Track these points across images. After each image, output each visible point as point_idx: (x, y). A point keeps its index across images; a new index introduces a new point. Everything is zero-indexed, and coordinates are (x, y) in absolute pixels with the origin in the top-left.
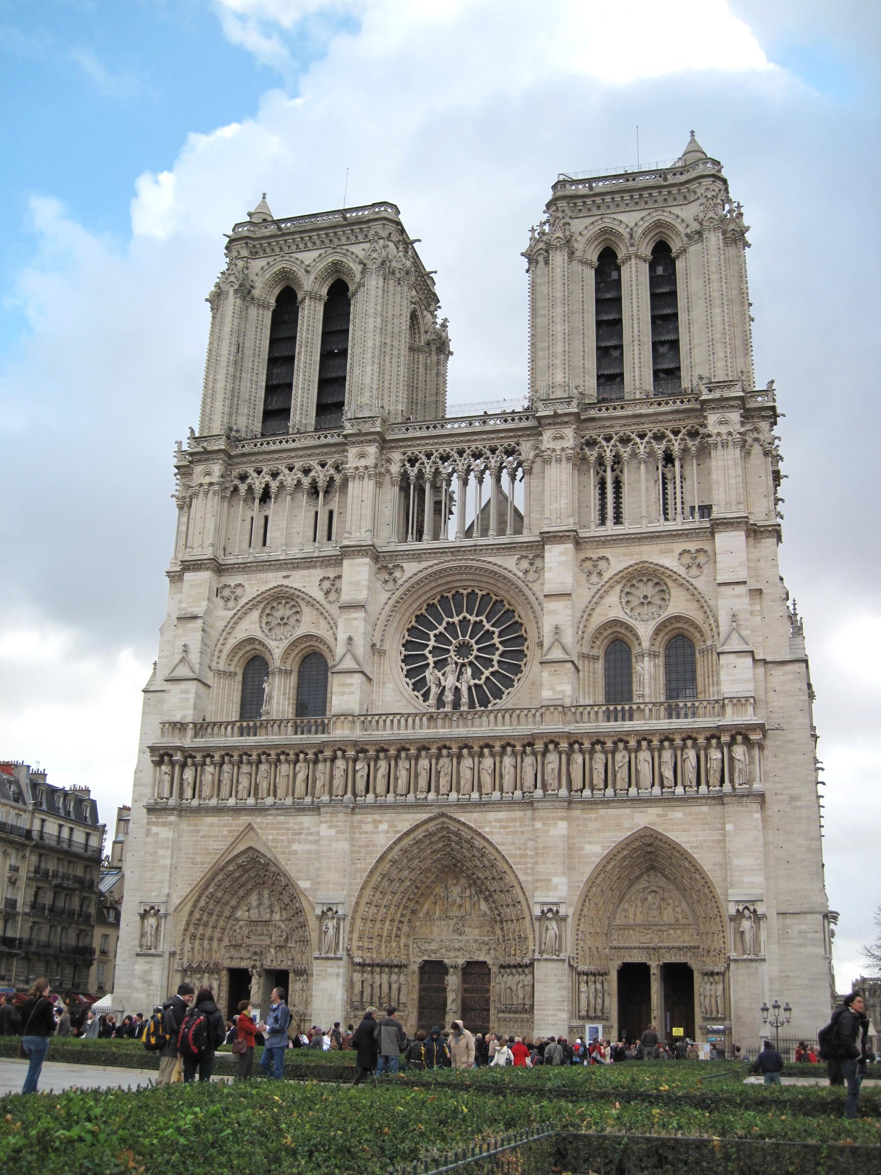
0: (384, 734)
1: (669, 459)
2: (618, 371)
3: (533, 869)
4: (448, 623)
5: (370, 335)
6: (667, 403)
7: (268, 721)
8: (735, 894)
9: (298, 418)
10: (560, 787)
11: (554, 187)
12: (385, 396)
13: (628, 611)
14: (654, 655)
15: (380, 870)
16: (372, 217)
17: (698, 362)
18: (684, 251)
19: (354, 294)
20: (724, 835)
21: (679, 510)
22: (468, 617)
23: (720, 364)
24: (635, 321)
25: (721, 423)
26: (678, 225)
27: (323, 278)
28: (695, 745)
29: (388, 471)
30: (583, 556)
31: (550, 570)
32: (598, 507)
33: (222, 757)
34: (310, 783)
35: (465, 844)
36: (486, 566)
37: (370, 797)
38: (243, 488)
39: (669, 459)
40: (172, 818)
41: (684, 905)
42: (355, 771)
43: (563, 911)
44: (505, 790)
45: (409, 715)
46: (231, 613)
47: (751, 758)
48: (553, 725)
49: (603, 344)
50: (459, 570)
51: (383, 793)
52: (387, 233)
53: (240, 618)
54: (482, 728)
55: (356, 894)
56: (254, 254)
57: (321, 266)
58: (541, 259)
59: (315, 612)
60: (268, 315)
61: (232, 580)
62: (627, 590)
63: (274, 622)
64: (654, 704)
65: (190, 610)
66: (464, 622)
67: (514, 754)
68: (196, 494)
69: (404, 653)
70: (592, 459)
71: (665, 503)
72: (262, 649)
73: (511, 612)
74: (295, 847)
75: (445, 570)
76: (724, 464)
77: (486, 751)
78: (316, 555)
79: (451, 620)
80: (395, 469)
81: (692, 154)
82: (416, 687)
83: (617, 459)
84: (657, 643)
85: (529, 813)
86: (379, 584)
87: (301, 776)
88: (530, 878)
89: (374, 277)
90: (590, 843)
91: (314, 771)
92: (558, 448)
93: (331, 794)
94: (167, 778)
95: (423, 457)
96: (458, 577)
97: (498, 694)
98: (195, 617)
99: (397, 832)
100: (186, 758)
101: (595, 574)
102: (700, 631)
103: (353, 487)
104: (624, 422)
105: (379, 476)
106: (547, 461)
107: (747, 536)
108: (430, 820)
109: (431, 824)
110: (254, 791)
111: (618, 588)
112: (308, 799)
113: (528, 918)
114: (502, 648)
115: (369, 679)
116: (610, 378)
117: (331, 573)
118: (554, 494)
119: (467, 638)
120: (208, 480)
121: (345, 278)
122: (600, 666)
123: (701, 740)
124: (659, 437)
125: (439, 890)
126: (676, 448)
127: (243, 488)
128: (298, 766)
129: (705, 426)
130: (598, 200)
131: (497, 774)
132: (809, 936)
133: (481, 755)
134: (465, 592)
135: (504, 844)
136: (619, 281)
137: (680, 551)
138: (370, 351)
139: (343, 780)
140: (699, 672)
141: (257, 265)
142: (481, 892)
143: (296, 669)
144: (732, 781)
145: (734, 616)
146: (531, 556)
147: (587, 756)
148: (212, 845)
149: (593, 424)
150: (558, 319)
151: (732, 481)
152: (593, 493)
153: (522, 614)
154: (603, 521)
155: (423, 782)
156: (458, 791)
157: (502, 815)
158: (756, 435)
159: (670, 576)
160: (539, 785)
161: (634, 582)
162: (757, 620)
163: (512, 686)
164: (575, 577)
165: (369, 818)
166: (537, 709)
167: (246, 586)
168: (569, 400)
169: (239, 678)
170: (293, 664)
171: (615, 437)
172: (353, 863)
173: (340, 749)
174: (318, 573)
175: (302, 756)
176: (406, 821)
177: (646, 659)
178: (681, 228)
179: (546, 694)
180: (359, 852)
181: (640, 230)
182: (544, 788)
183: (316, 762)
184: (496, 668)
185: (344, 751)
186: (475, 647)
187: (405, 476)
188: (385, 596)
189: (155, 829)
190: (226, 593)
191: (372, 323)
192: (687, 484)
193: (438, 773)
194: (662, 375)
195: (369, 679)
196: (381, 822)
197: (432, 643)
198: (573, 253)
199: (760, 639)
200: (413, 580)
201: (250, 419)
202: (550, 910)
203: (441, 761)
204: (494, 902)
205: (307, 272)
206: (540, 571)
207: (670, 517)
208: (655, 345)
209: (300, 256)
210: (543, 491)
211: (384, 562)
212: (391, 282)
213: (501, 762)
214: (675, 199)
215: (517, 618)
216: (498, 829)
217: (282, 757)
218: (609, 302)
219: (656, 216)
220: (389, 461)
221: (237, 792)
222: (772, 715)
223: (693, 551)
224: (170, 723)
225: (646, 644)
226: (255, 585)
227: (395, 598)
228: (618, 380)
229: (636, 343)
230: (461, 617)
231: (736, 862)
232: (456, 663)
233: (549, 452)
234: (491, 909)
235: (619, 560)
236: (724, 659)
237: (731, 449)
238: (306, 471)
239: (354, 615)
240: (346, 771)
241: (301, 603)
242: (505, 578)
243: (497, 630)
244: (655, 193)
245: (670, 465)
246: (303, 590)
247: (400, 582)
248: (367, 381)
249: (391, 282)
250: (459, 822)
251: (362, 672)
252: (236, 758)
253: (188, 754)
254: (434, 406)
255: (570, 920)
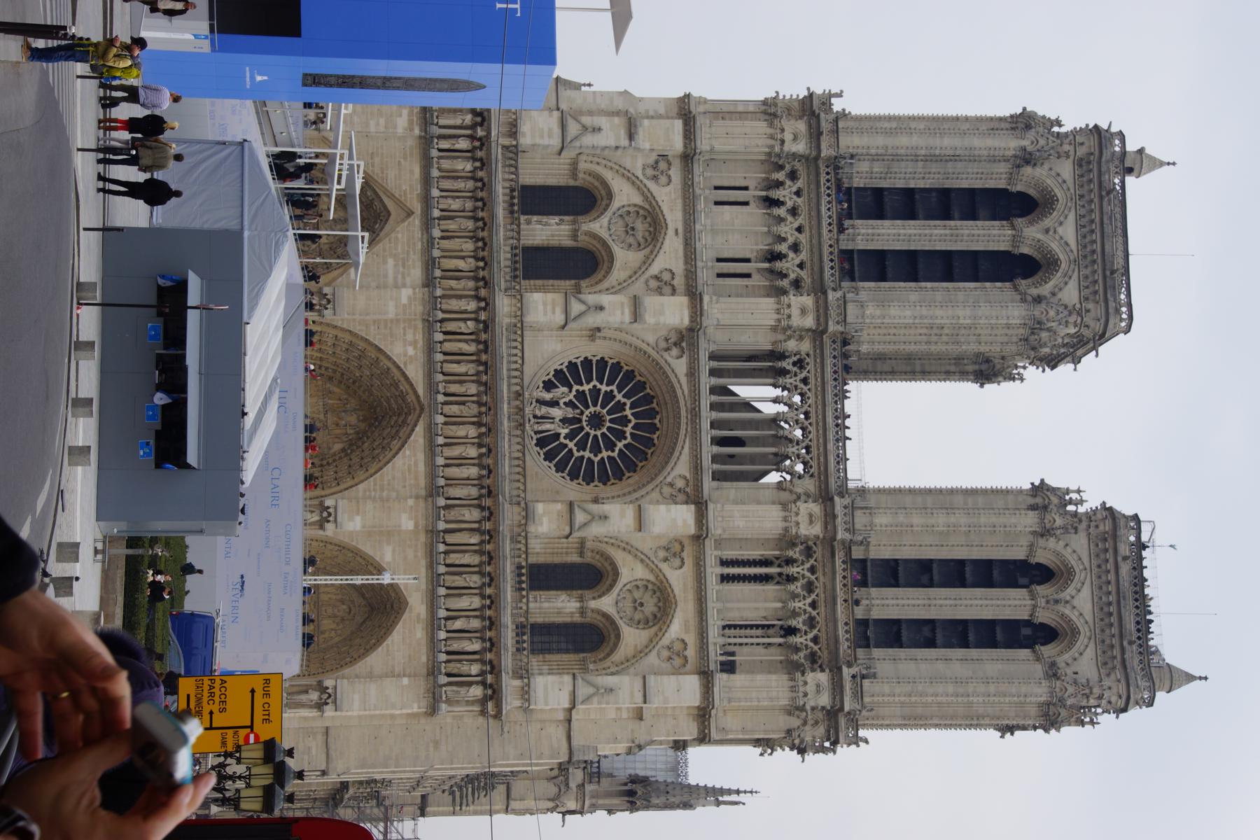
0: (503, 347)
1: (791, 631)
2: (901, 580)
3: (370, 497)
4: (625, 404)
5: (950, 312)
6: (847, 632)
7: (519, 226)
8: (343, 685)
9: (863, 231)
10: (446, 522)
11: (1136, 518)
12: (879, 331)
13: (628, 587)
14: (582, 611)
15: (369, 348)
16: (1112, 305)
17: (896, 668)
18: (1038, 660)
19: (1016, 289)
20: (399, 676)
21: (732, 640)
22: (630, 425)
23: (887, 689)
24: (952, 602)
25: (818, 686)
26: (1071, 653)
27: (1040, 246)
28: (484, 650)
29: (789, 338)
30: (686, 542)
31: (668, 511)
32: (740, 558)
33: (481, 180)
34: (455, 274)
35: (394, 431)
36: (680, 444)
37: (439, 337)
38: (780, 176)
39: (791, 631)
40: (417, 132)
41: (337, 639)
42: (465, 320)
43: (330, 527)
44: (447, 469)
45: (522, 373)
46: (639, 174)
47: (473, 703)
48: (509, 516)
49: (935, 566)
50: (678, 416)
51: (444, 349)
52: (1092, 324)
53: (633, 183)
54: (507, 446)
55: (345, 326)
56: (1080, 163)
57: (1055, 246)
58: (1038, 500)
59: (637, 265)
60: (1002, 185)
61: (676, 173)
62: (650, 586)
63: (629, 220)
64: (527, 612)
65: (640, 131)
66: (625, 421)
67: (481, 477)
68: (771, 125)
69: (594, 360)
70: (790, 553)
71: (741, 627)
72: (603, 206)
73: (632, 467)
74: (391, 262)
75: (678, 401)
76: (774, 687)
77: (484, 450)
78: (699, 264)
79: (627, 407)
80: (792, 345)
81: (1168, 676)
82: (558, 373)
83: (790, 579)
84: (595, 615)
85: (423, 493)
86: (664, 333)
87: (461, 264)
88: (361, 494)
89: (1024, 313)
90: (394, 551)
91: (468, 278)
92: (800, 519)
93: (443, 297)
94: (458, 122)
95: (803, 375)
96: (671, 415)
97: (549, 457)
98: (631, 137)
99: (405, 364)
100: (480, 139)
101: (666, 554)
102: (605, 658)
103: (769, 303)
104: (829, 586)
105: (782, 328)
106: (785, 506)
107: (698, 707)
108: (418, 397)
109: (413, 398)
110: (448, 215)
111: (652, 578)
112: (438, 273)
113: (323, 493)
114: (596, 460)
115: (563, 327)
116: (893, 573)
117: (679, 282)
118: (752, 515)
119: (608, 424)
120: (788, 136)
121: (1040, 273)
122: (575, 558)
123: (489, 656)
124: (811, 623)
125: (353, 403)
126: (797, 640)
127: (780, 176)
128: (471, 260)
129: (813, 670)
130: (1110, 566)
131: (460, 461)
132: (306, 757)
133: (480, 446)
134: (657, 421)
135: (393, 468)
136: (1016, 585)
137: (687, 640)
138: (931, 313)
139: (456, 308)
140: (565, 657)
141: (1066, 169)
142: (351, 445)
143: (580, 245)
144: (450, 684)
145: (611, 690)
146: (688, 490)
147: (476, 548)
148: (391, 174)
149: (828, 554)
150: (952, 519)
151: (754, 695)
152: (756, 554)
153: (630, 481)
154: (724, 563)
155: (454, 388)
156: (445, 424)
157: (422, 467)
158: (810, 722)
159: (661, 629)
160: (449, 502)
161: (658, 594)
162: (612, 715)
163: (557, 471)
164: (659, 537)
165: (419, 337)
166: (525, 499)
167: (668, 189)
168: (851, 530)
169: (572, 183)
170: (583, 241)
171: (813, 578)
172: (374, 321)
173: (487, 304)
174: (679, 267)
175: (481, 264)
176: (416, 373)
177: (578, 605)
178: (1066, 656)
179: (540, 508)
180: (386, 327)
181: (1067, 612)
182: (446, 507)
183: (476, 279)
184: (576, 454)
185: (485, 309)
186: (599, 433)
187: (782, 356)
188: (651, 339)
189: (405, 112)
190: (663, 165)
191: (964, 315)
192: (761, 649)
193: (463, 403)
194: (895, 629)
195: (563, 327)
196: (415, 348)
197: (604, 388)
198: (1042, 536)
199: (593, 716)
200: (667, 369)
201: (861, 176)
202: (330, 515)
203: (475, 406)
204: (340, 458)
205: (1047, 231)
206: (673, 500)
207: (727, 631)
208: (931, 622)
209: (1072, 217)
210: (759, 503)
211: (687, 338)
212: (1022, 331)
213: (474, 465)
214: (1104, 652)
215: (627, 475)
216: (409, 462)
217: (480, 244)
218: (987, 573)
219: (1084, 631)
220: (801, 338)
221: (446, 197)
222: (518, 727)
223: (686, 653)
224: (516, 120)
225: (593, 604)
226: (668, 198)
227: (649, 350)
228: (893, 581)
229: (926, 602)
230: (630, 417)
231: (373, 688)
232: (582, 413)
233: (794, 509)
234: (334, 454)
235: (679, 579)
236: (567, 679)
237: (788, 694)
238: (795, 248)
239: (627, 311)
240: (465, 312)
241: (648, 250)
242: (667, 463)
243: (615, 454)
244: (1115, 630)
245: (782, 633)
246: (662, 252)
247: (666, 355)
248: (893, 311)
249: (1022, 331)
250: (415, 425)
251: (566, 324)
252: (480, 194)
253: (484, 142)
254: (909, 369)
255: (321, 532)
